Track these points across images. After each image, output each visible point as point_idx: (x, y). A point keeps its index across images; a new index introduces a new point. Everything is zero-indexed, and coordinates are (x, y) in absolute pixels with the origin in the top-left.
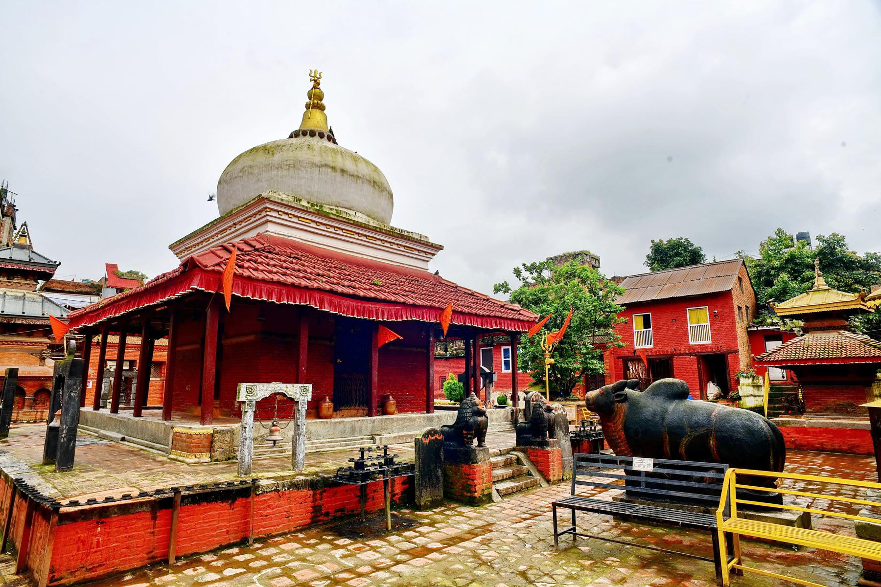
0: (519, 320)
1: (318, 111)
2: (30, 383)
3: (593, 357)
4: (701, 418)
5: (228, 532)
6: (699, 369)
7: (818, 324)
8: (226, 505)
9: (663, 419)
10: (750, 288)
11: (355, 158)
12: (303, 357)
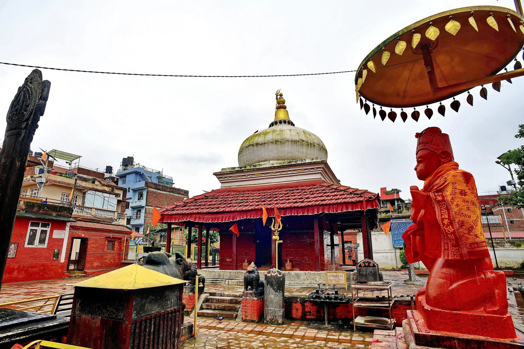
1: (283, 110)
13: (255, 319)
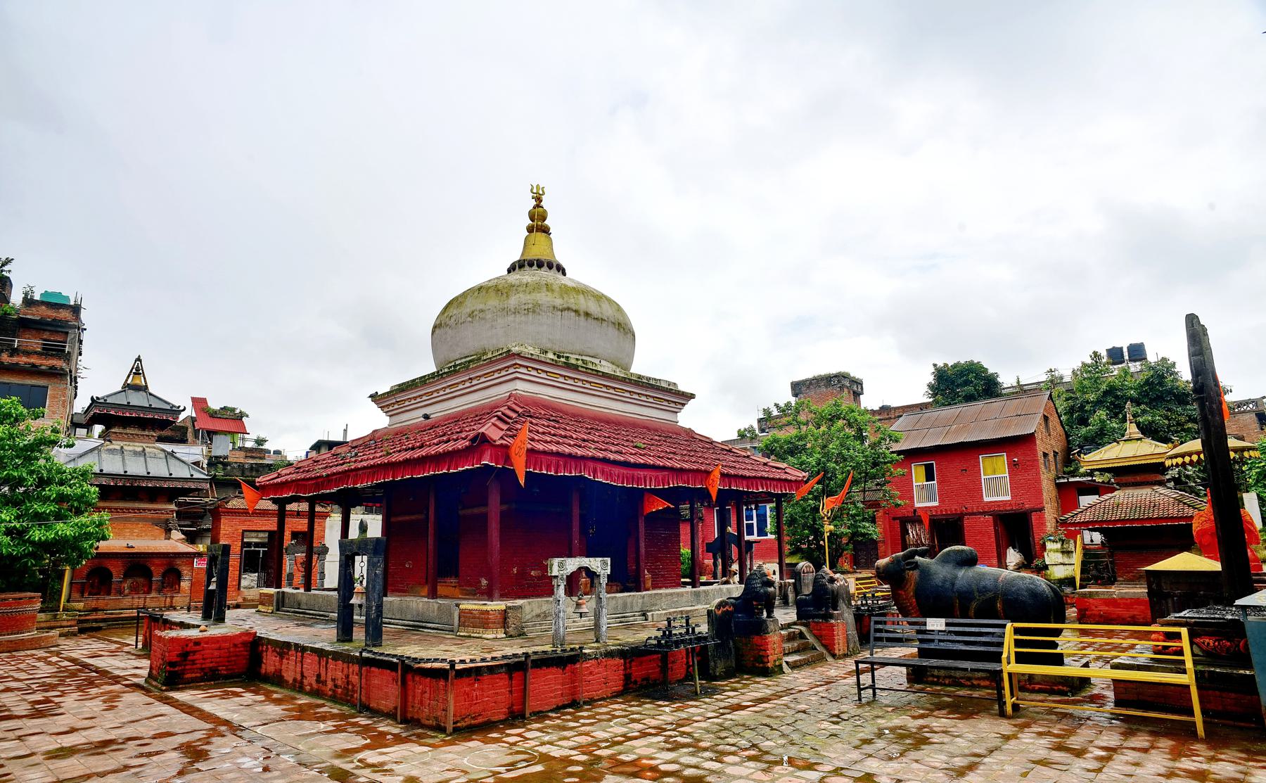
0: (786, 480)
2: (157, 561)
3: (863, 520)
4: (988, 583)
6: (996, 531)
7: (1130, 479)
9: (953, 584)
10: (1059, 428)
11: (599, 297)
12: (576, 529)
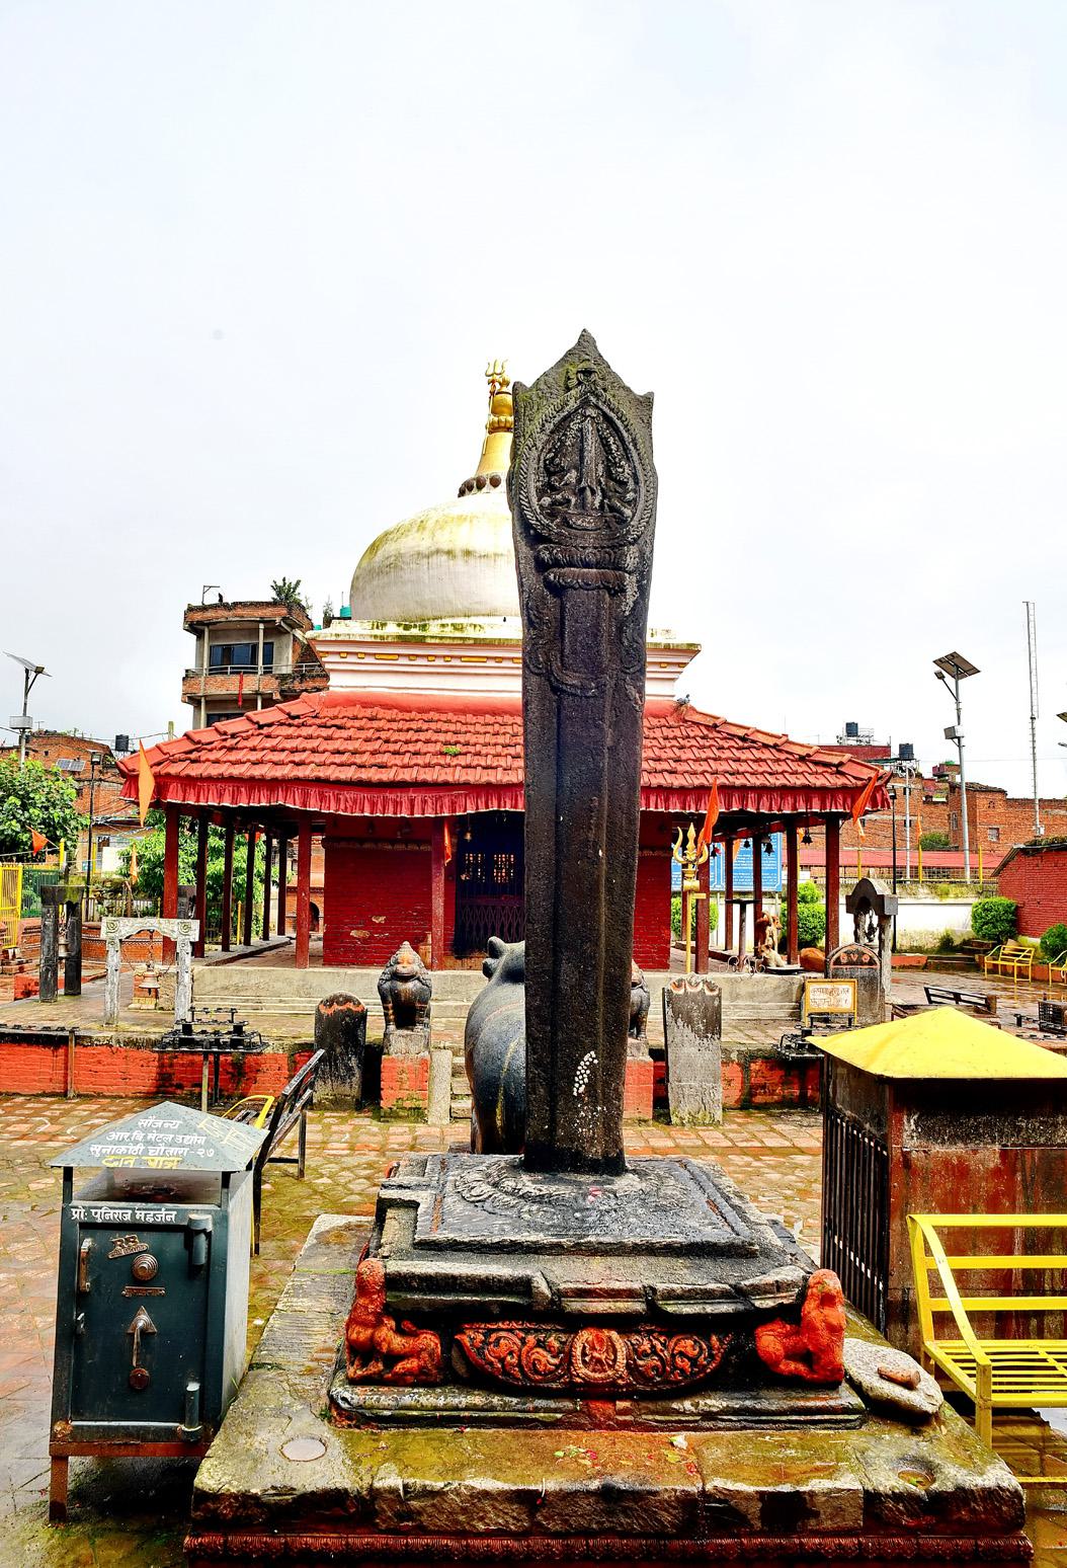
5: (51, 1080)
8: (48, 1051)
13: (648, 1113)
